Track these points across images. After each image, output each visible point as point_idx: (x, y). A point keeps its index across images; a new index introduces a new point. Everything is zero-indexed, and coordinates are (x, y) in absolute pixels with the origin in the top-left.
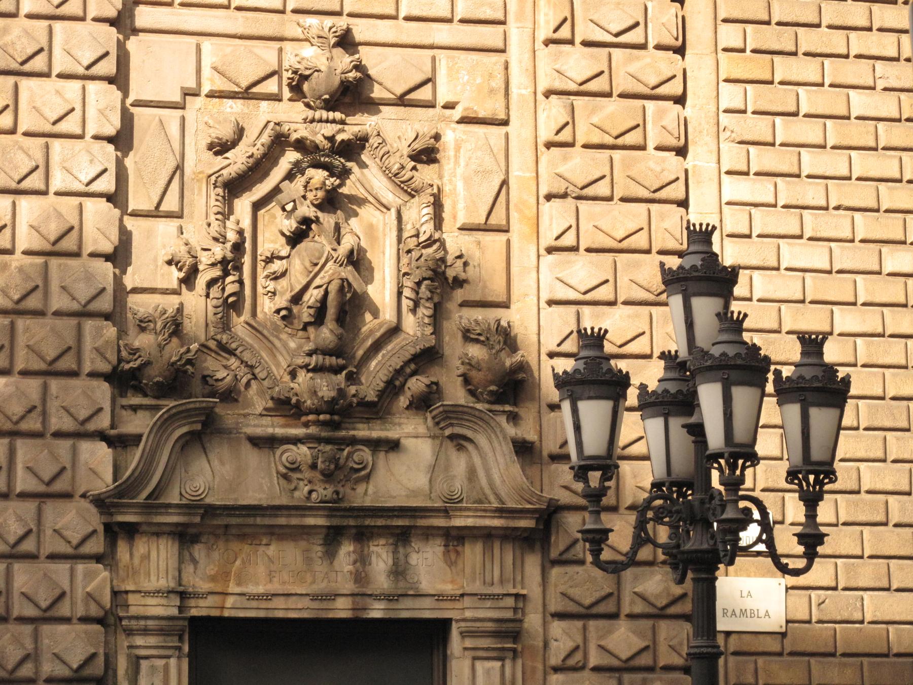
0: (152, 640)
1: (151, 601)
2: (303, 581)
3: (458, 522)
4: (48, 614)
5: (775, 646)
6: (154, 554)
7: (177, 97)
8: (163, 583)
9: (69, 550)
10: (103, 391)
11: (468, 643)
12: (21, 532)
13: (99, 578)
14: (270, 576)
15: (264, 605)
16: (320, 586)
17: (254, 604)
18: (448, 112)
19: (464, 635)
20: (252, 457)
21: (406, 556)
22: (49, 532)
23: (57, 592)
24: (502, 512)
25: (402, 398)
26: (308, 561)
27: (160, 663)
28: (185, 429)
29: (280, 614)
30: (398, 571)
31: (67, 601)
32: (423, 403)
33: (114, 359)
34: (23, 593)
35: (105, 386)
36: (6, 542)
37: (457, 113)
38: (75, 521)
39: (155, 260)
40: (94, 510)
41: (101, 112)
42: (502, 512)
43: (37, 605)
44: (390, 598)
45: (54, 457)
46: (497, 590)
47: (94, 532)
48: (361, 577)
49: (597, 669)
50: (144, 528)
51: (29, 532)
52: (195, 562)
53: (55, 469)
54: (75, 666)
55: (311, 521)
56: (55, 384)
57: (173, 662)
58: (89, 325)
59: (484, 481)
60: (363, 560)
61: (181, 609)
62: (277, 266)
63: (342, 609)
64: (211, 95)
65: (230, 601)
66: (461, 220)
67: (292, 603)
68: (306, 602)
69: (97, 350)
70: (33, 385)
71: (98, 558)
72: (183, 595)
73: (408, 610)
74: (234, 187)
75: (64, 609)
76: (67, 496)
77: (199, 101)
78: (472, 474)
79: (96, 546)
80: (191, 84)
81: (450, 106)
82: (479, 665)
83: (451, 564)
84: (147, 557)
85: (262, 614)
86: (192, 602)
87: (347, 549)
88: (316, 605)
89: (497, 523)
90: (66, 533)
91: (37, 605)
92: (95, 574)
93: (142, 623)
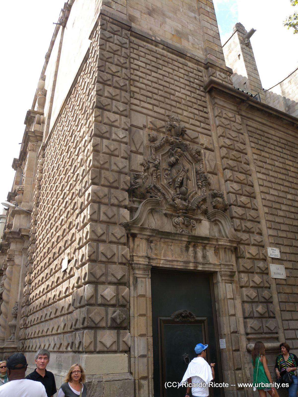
0: (141, 272)
1: (141, 259)
2: (181, 257)
3: (220, 243)
4: (110, 260)
5: (284, 282)
6: (141, 245)
7: (142, 126)
8: (144, 254)
9: (116, 241)
10: (126, 194)
11: (223, 278)
12: (102, 232)
13: (126, 250)
14: (172, 255)
15: (171, 263)
16: (185, 259)
17: (168, 263)
18: (202, 146)
19: (221, 276)
20: (165, 220)
21: (206, 253)
22: (110, 234)
23: (113, 253)
24: (230, 241)
25: (199, 211)
26: (182, 251)
27: (144, 280)
28: (150, 208)
29: (175, 267)
30: (204, 257)
31: (116, 257)
32: (205, 213)
33: (129, 185)
34: (102, 253)
35: (127, 193)
36: (97, 235)
37: (204, 146)
38: (119, 232)
39: (138, 163)
40: (124, 229)
41: (125, 122)
42: (230, 241)
43: (106, 257)
44: (203, 264)
45: (113, 211)
46: (229, 263)
47: (124, 235)
48: (195, 257)
49: (252, 287)
50: (139, 236)
51: (104, 233)
52: (151, 248)
53: (113, 214)
54: (119, 278)
55: (184, 239)
56: (112, 190)
57: (147, 279)
58: (122, 176)
59: (223, 233)
60: (195, 253)
61: (149, 262)
62: (167, 172)
63: (191, 267)
64: (149, 128)
65: (162, 262)
66: (208, 169)
67: (178, 264)
68: (181, 264)
69: (124, 182)
70: (106, 190)
71: (124, 244)
72: (149, 258)
73: (208, 268)
74: (157, 149)
75: (115, 259)
76: (115, 224)
77: (147, 129)
78: (220, 231)
79: (124, 240)
80: (145, 124)
81: (202, 145)
82: (227, 284)
83: (216, 256)
84: (138, 246)
85: (171, 266)
86: (151, 261)
87: (191, 249)
88: (185, 265)
89: (229, 244)
90: (115, 234)
91: (106, 257)
92: (125, 249)
93: (139, 266)
